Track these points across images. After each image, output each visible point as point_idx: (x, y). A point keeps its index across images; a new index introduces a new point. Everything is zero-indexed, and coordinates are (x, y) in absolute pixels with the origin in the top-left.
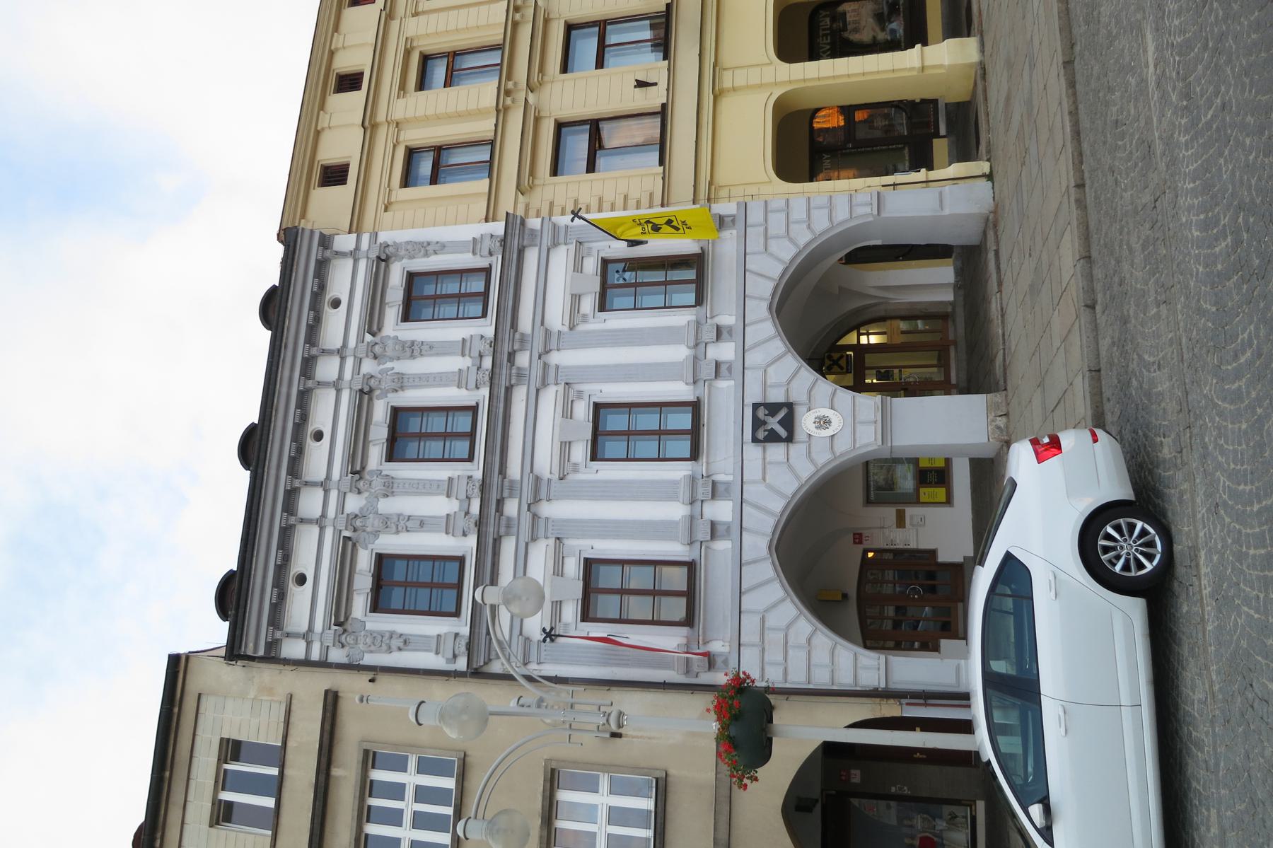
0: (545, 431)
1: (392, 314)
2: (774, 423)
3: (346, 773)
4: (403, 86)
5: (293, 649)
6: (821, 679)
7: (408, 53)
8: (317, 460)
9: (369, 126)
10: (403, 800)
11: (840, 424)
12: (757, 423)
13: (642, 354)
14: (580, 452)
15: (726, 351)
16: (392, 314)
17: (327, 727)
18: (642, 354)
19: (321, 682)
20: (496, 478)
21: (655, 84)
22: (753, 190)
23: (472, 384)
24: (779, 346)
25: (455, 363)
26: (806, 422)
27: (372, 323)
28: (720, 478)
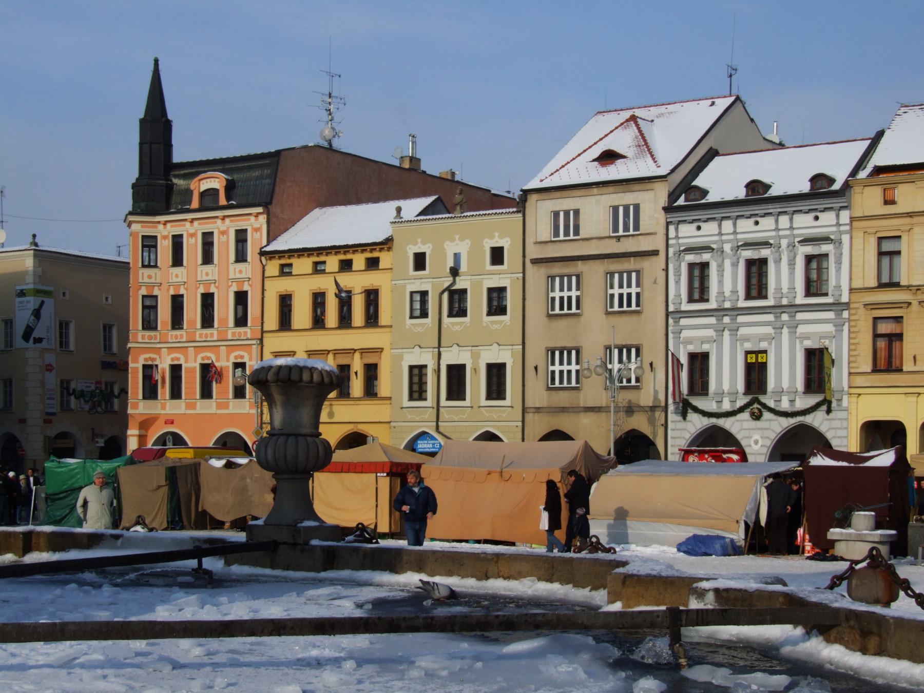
0: (755, 330)
1: (809, 249)
3: (631, 264)
5: (672, 233)
8: (745, 225)
14: (748, 346)
16: (809, 249)
19: (661, 248)
22: (854, 412)
27: (806, 241)
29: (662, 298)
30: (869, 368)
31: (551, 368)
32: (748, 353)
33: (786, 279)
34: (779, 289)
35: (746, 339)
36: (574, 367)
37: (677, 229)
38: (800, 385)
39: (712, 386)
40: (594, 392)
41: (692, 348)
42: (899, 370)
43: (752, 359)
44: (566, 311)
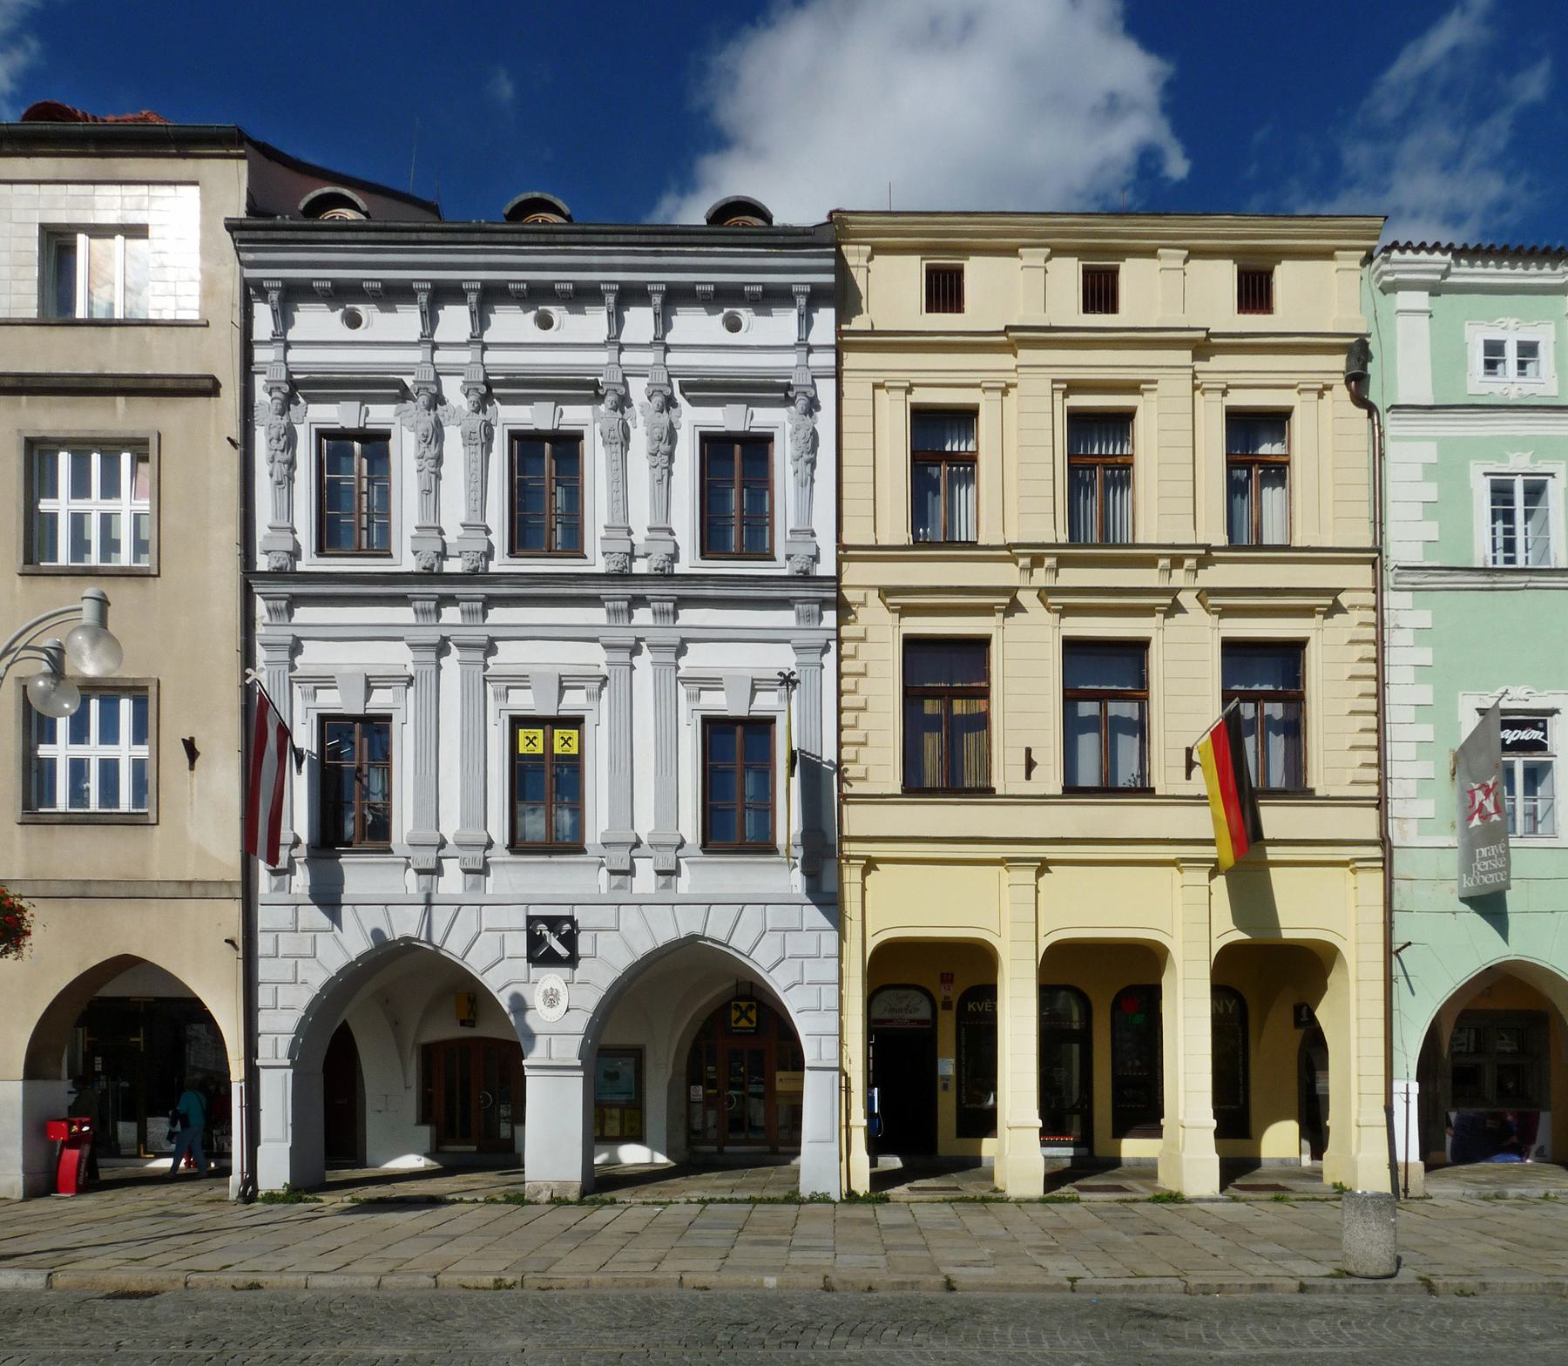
0: (545, 652)
2: (552, 941)
3: (118, 417)
4: (1073, 387)
6: (264, 996)
7: (1133, 388)
9: (1015, 339)
11: (556, 1015)
12: (553, 922)
14: (524, 702)
15: (645, 881)
17: (169, 384)
18: (644, 779)
21: (1028, 777)
23: (611, 547)
24: (644, 946)
25: (641, 517)
26: (552, 978)
27: (705, 389)
29: (230, 532)
31: (143, 751)
32: (517, 723)
33: (639, 498)
35: (519, 681)
36: (126, 751)
37: (284, 318)
38: (690, 825)
39: (404, 823)
41: (331, 701)
42: (1142, 790)
43: (532, 742)
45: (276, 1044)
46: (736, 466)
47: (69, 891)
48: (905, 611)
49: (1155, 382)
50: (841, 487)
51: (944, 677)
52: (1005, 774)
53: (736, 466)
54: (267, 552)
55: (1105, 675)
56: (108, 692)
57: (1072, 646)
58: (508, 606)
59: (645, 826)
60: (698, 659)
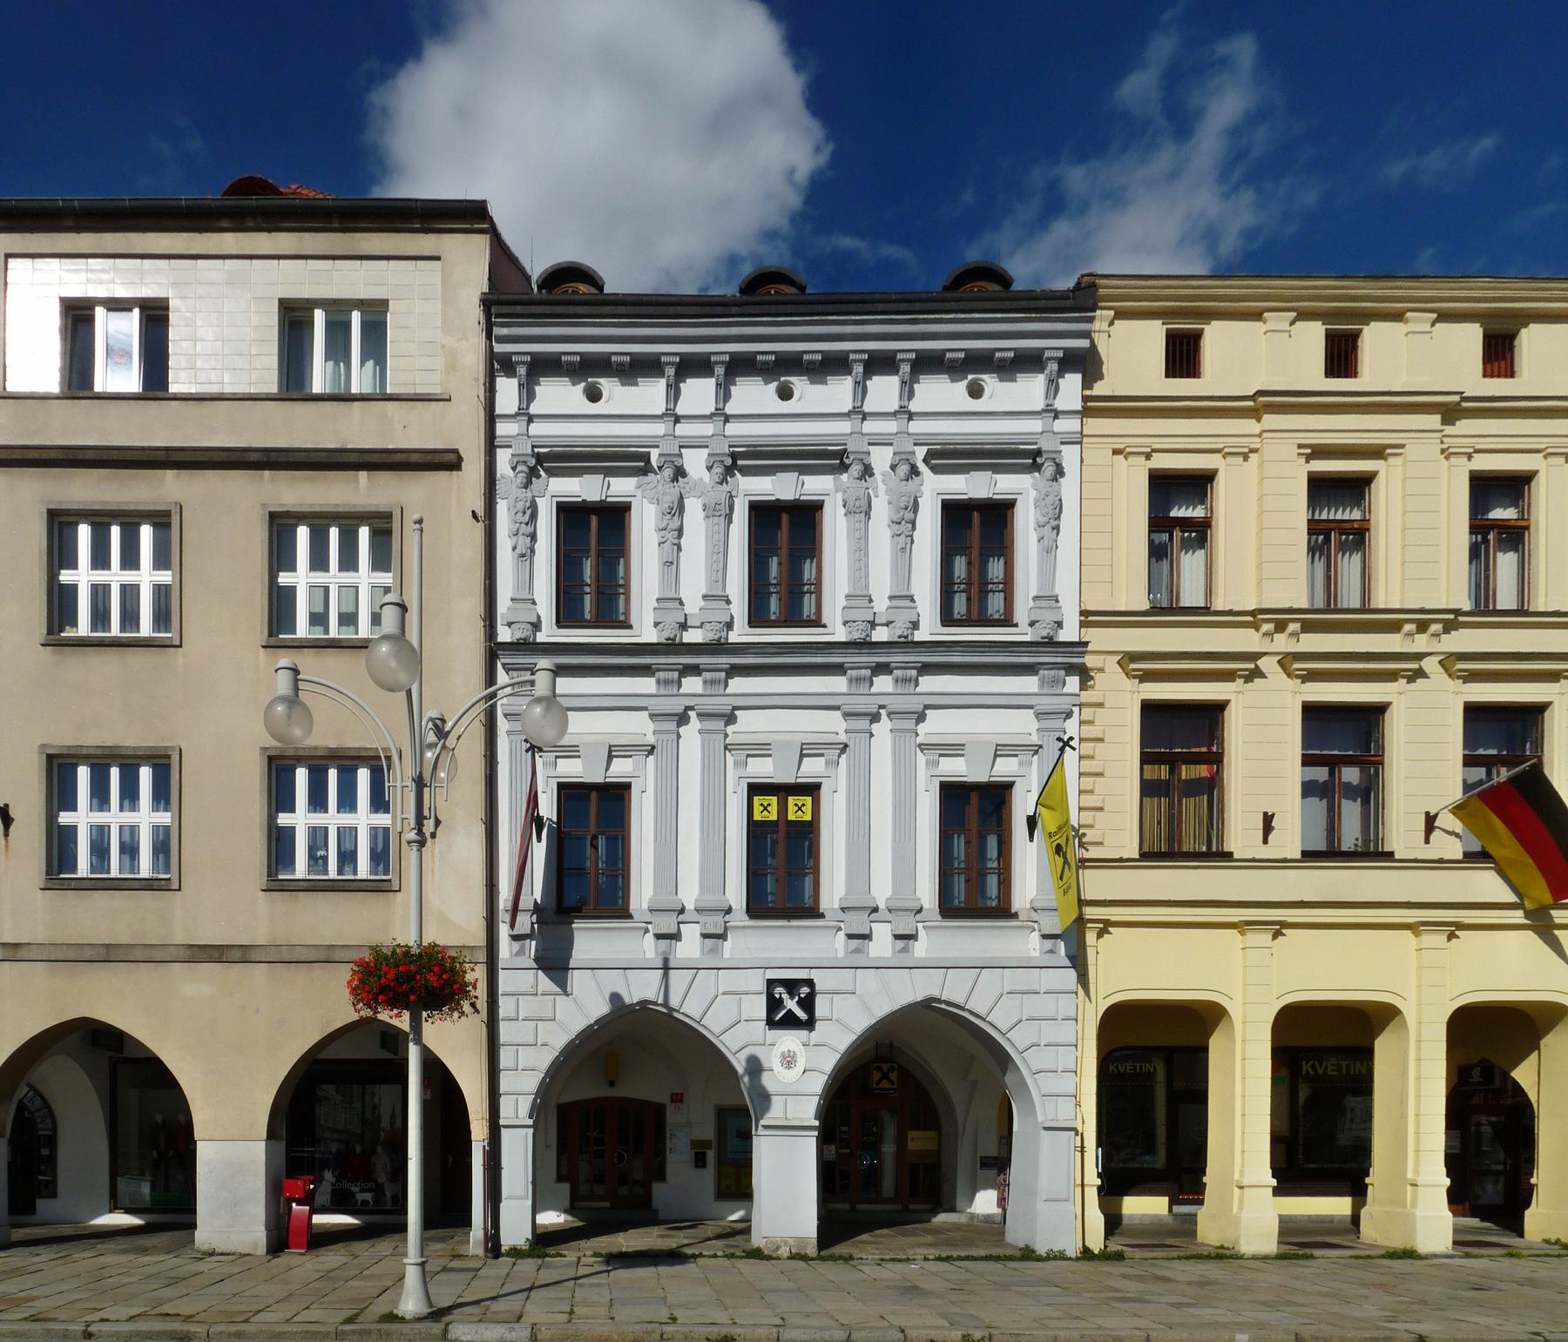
0: (784, 721)
2: (792, 1004)
3: (361, 491)
4: (1318, 452)
6: (505, 1058)
7: (1378, 452)
10: (340, 570)
12: (791, 986)
13: (880, 844)
14: (763, 769)
15: (882, 944)
17: (414, 458)
18: (880, 844)
20: (726, 660)
21: (1265, 841)
23: (852, 615)
24: (883, 1007)
25: (881, 587)
26: (790, 1040)
27: (947, 457)
28: (727, 945)
29: (474, 603)
30: (1129, 847)
32: (755, 789)
33: (879, 565)
34: (859, 597)
35: (760, 749)
37: (527, 392)
38: (927, 891)
39: (643, 890)
40: (223, 893)
41: (572, 770)
43: (768, 810)
44: (115, 630)
45: (517, 1107)
46: (977, 532)
47: (313, 955)
48: (1147, 677)
49: (1402, 446)
50: (1079, 552)
51: (1182, 742)
52: (1240, 835)
53: (977, 532)
54: (509, 624)
55: (1344, 742)
56: (348, 762)
57: (1312, 712)
58: (748, 675)
59: (882, 892)
60: (937, 725)
